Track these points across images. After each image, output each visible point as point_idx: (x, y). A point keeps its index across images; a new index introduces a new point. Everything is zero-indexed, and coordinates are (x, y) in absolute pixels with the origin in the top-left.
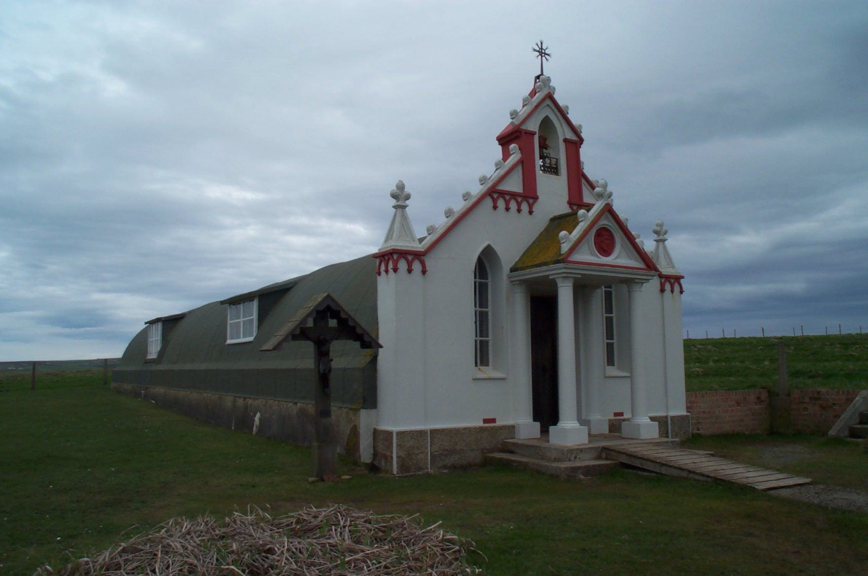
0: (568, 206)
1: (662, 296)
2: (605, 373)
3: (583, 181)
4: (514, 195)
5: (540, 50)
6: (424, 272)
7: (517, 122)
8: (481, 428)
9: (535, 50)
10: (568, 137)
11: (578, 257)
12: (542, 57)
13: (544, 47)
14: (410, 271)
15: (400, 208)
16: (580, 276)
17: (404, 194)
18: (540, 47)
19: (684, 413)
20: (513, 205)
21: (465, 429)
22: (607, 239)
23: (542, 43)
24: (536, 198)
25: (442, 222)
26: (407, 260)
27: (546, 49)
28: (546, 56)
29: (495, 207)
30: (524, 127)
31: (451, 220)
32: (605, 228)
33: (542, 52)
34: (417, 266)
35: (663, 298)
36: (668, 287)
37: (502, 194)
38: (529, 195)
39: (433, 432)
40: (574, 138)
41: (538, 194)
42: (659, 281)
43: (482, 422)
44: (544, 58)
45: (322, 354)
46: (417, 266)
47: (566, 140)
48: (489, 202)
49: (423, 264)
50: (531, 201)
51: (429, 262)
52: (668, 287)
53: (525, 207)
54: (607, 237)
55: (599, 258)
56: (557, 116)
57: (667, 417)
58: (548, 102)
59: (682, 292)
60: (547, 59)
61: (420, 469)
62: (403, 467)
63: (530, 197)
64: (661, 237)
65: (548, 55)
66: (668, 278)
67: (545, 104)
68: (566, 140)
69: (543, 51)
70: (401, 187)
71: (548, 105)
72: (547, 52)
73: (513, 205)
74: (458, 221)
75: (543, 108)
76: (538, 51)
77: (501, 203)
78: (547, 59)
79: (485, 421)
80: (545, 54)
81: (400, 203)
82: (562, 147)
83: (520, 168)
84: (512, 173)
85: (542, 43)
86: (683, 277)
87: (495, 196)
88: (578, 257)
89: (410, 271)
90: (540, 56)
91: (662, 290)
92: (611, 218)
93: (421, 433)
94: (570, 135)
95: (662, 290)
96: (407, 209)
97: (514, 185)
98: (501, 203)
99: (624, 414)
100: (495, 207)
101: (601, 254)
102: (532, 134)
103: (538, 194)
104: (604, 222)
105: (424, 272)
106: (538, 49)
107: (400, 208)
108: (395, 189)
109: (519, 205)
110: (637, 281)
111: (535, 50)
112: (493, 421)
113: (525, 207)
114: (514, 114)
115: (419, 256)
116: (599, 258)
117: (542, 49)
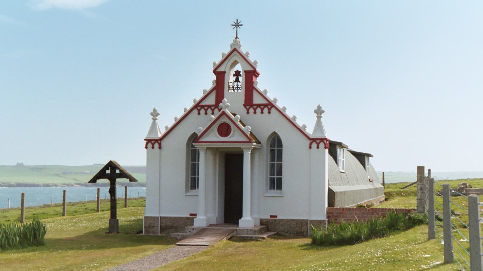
0: (244, 107)
3: (254, 92)
4: (209, 106)
5: (236, 24)
6: (160, 148)
8: (187, 218)
12: (237, 27)
13: (238, 22)
14: (153, 148)
16: (205, 148)
17: (156, 113)
18: (236, 22)
21: (178, 217)
27: (240, 22)
28: (240, 26)
29: (199, 114)
30: (219, 70)
31: (177, 121)
34: (156, 145)
36: (314, 145)
37: (203, 107)
39: (161, 217)
40: (251, 69)
42: (309, 142)
43: (189, 215)
44: (238, 28)
46: (156, 145)
48: (196, 111)
51: (164, 143)
52: (314, 145)
55: (218, 137)
57: (307, 220)
58: (235, 53)
61: (155, 233)
62: (147, 232)
64: (319, 115)
65: (241, 25)
66: (314, 140)
69: (238, 24)
70: (155, 110)
71: (235, 55)
72: (240, 24)
75: (234, 55)
76: (235, 25)
77: (202, 111)
80: (239, 25)
83: (214, 92)
84: (211, 94)
85: (237, 21)
87: (199, 108)
89: (153, 148)
90: (236, 28)
91: (310, 147)
93: (156, 218)
94: (249, 68)
95: (310, 147)
97: (211, 100)
98: (202, 111)
99: (278, 217)
100: (199, 114)
101: (221, 136)
104: (224, 120)
105: (160, 148)
106: (234, 24)
110: (241, 148)
113: (216, 111)
114: (214, 64)
117: (237, 23)
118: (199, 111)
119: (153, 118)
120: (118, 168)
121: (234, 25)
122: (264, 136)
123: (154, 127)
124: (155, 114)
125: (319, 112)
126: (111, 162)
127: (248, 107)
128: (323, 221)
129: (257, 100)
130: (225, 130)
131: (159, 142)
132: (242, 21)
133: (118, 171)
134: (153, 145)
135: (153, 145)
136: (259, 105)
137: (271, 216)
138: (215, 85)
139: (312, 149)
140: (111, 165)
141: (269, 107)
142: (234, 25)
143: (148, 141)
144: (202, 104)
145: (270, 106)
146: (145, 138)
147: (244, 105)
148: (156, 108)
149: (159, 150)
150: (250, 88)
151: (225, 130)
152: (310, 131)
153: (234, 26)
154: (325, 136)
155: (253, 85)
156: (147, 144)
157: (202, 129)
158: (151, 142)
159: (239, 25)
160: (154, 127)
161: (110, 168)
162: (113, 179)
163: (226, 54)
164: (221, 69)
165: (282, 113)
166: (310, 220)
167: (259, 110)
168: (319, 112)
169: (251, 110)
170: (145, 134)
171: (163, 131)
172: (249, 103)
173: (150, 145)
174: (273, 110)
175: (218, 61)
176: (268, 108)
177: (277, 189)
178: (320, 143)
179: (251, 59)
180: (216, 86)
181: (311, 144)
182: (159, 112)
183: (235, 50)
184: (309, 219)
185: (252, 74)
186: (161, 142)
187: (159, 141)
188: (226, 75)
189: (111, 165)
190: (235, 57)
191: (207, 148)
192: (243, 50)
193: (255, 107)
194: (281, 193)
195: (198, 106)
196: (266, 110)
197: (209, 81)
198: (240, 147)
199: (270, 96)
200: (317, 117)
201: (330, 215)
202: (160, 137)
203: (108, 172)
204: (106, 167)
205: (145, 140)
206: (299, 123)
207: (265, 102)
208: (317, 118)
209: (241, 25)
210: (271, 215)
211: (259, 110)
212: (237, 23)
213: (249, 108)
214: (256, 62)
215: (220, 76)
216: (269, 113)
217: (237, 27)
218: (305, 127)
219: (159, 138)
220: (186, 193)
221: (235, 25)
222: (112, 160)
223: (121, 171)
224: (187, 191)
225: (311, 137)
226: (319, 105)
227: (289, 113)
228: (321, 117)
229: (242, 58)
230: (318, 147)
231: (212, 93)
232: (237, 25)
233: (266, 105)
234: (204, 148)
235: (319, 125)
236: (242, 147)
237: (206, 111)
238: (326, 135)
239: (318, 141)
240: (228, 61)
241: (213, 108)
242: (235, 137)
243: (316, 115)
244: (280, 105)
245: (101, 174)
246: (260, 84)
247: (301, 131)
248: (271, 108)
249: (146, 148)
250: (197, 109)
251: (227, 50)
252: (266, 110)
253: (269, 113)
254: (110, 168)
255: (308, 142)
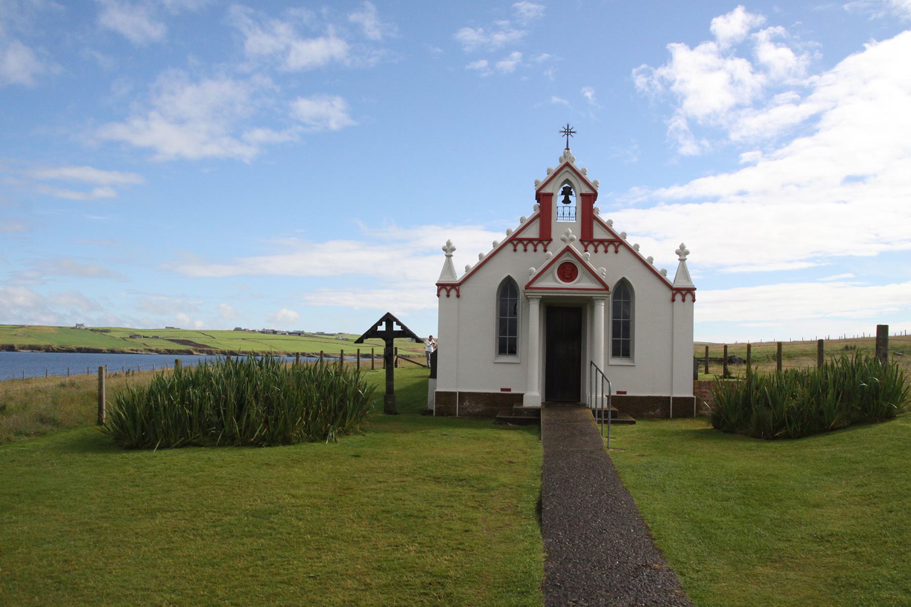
1: (673, 304)
2: (608, 362)
3: (595, 223)
4: (530, 240)
6: (458, 296)
7: (537, 189)
9: (561, 132)
10: (584, 192)
11: (540, 284)
12: (568, 135)
13: (570, 128)
14: (448, 296)
15: (449, 257)
16: (541, 297)
17: (451, 247)
18: (566, 128)
19: (691, 395)
20: (530, 247)
22: (568, 270)
23: (568, 126)
24: (550, 240)
25: (474, 262)
26: (446, 289)
28: (571, 134)
29: (515, 250)
30: (542, 191)
32: (571, 263)
33: (568, 132)
34: (453, 293)
35: (673, 307)
38: (545, 237)
39: (460, 393)
40: (589, 191)
41: (553, 236)
44: (569, 136)
45: (389, 345)
46: (453, 293)
47: (581, 195)
48: (510, 247)
49: (458, 291)
50: (545, 243)
51: (463, 290)
52: (678, 297)
53: (540, 247)
54: (568, 269)
55: (560, 283)
56: (575, 177)
57: (669, 397)
58: (567, 169)
59: (694, 300)
60: (572, 136)
63: (544, 240)
64: (683, 257)
65: (574, 132)
66: (679, 290)
67: (565, 170)
68: (581, 195)
69: (569, 131)
71: (567, 171)
72: (572, 131)
73: (530, 247)
74: (485, 262)
76: (565, 132)
78: (572, 136)
79: (502, 390)
80: (571, 132)
81: (448, 254)
82: (580, 198)
83: (538, 222)
84: (532, 224)
85: (568, 126)
86: (695, 289)
87: (515, 242)
88: (540, 284)
89: (448, 296)
91: (673, 300)
92: (572, 256)
94: (586, 190)
95: (673, 300)
96: (452, 258)
97: (533, 232)
98: (520, 247)
100: (515, 250)
102: (552, 195)
103: (552, 238)
104: (566, 258)
105: (458, 296)
107: (449, 257)
108: (446, 245)
109: (535, 246)
110: (593, 298)
111: (561, 132)
112: (509, 390)
113: (540, 247)
114: (537, 183)
115: (453, 286)
116: (560, 283)
117: (568, 129)
118: (515, 246)
119: (447, 254)
120: (399, 323)
121: (564, 132)
122: (612, 283)
123: (449, 267)
124: (449, 250)
125: (682, 253)
126: (388, 314)
127: (586, 243)
128: (693, 398)
129: (598, 233)
130: (568, 271)
131: (457, 288)
132: (574, 126)
133: (397, 328)
134: (448, 292)
135: (448, 292)
136: (601, 241)
137: (618, 392)
138: (538, 212)
139: (674, 303)
140: (389, 319)
141: (617, 244)
142: (564, 132)
143: (441, 286)
144: (520, 236)
145: (617, 242)
146: (436, 282)
147: (580, 240)
148: (452, 241)
149: (457, 299)
150: (588, 217)
151: (568, 271)
152: (670, 277)
153: (564, 133)
154: (694, 286)
155: (593, 212)
156: (439, 291)
157: (535, 271)
158: (446, 288)
159: (571, 132)
160: (449, 267)
161: (384, 323)
162: (389, 336)
163: (554, 169)
164: (547, 190)
165: (633, 252)
166: (673, 398)
167: (601, 248)
168: (682, 253)
169: (591, 248)
170: (436, 278)
171: (460, 273)
172: (587, 238)
173: (444, 292)
174: (621, 249)
175: (543, 177)
176: (614, 245)
177: (622, 355)
178: (686, 294)
179: (590, 178)
180: (540, 213)
181: (674, 295)
182: (454, 245)
183: (567, 165)
184: (672, 396)
185: (589, 199)
186: (459, 288)
187: (455, 286)
188: (553, 198)
189: (389, 319)
190: (565, 176)
191: (542, 296)
192: (578, 165)
193: (596, 243)
194: (634, 363)
195: (514, 240)
196: (611, 248)
197: (529, 208)
198: (592, 297)
199: (617, 229)
200: (679, 259)
201: (696, 390)
202: (457, 281)
203: (382, 328)
204: (380, 323)
205: (437, 285)
206: (657, 265)
207: (610, 237)
208: (679, 261)
209: (574, 132)
210: (618, 390)
211: (601, 248)
212: (568, 129)
213: (588, 245)
214: (596, 183)
215: (544, 199)
216: (616, 252)
217: (568, 135)
218: (665, 272)
219: (457, 283)
220: (495, 360)
221: (565, 132)
222: (390, 312)
223: (403, 327)
224: (496, 356)
225: (674, 287)
226: (682, 244)
227: (644, 253)
228: (686, 259)
229: (578, 178)
230: (684, 300)
231: (534, 222)
232: (568, 132)
233: (611, 242)
234: (539, 297)
235: (683, 270)
236: (594, 297)
237: (525, 246)
238: (693, 284)
239: (684, 292)
240: (557, 180)
241: (535, 243)
242: (582, 283)
243: (678, 257)
244: (631, 241)
245: (373, 333)
246: (604, 211)
247: (660, 277)
248: (619, 245)
249: (438, 295)
250: (513, 244)
251: (555, 165)
252: (611, 248)
253: (616, 252)
254: (384, 323)
255: (669, 294)
